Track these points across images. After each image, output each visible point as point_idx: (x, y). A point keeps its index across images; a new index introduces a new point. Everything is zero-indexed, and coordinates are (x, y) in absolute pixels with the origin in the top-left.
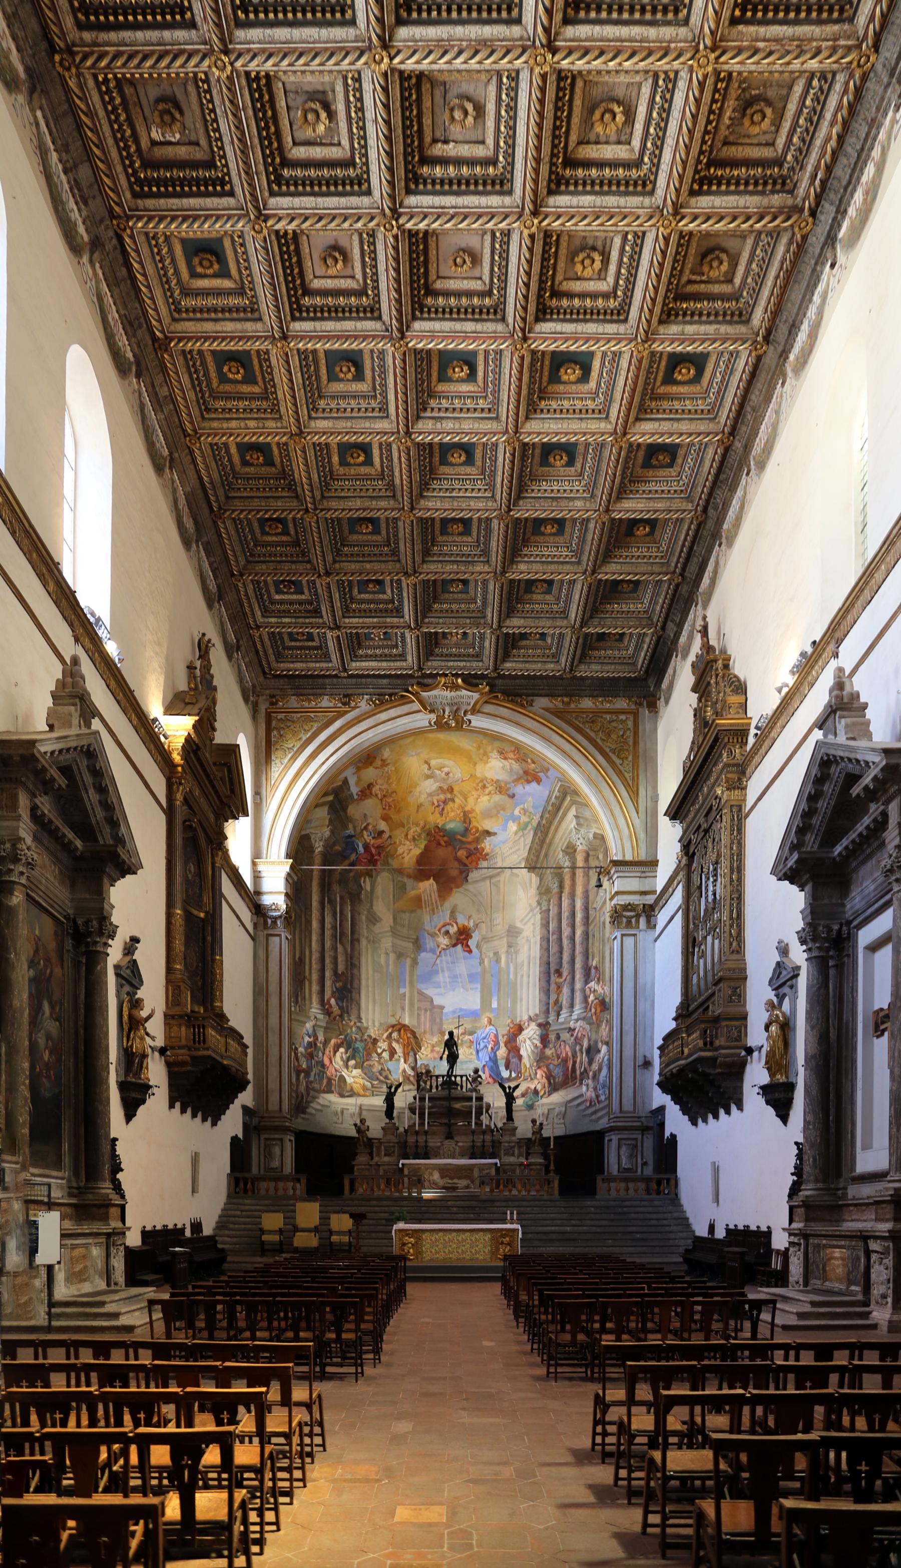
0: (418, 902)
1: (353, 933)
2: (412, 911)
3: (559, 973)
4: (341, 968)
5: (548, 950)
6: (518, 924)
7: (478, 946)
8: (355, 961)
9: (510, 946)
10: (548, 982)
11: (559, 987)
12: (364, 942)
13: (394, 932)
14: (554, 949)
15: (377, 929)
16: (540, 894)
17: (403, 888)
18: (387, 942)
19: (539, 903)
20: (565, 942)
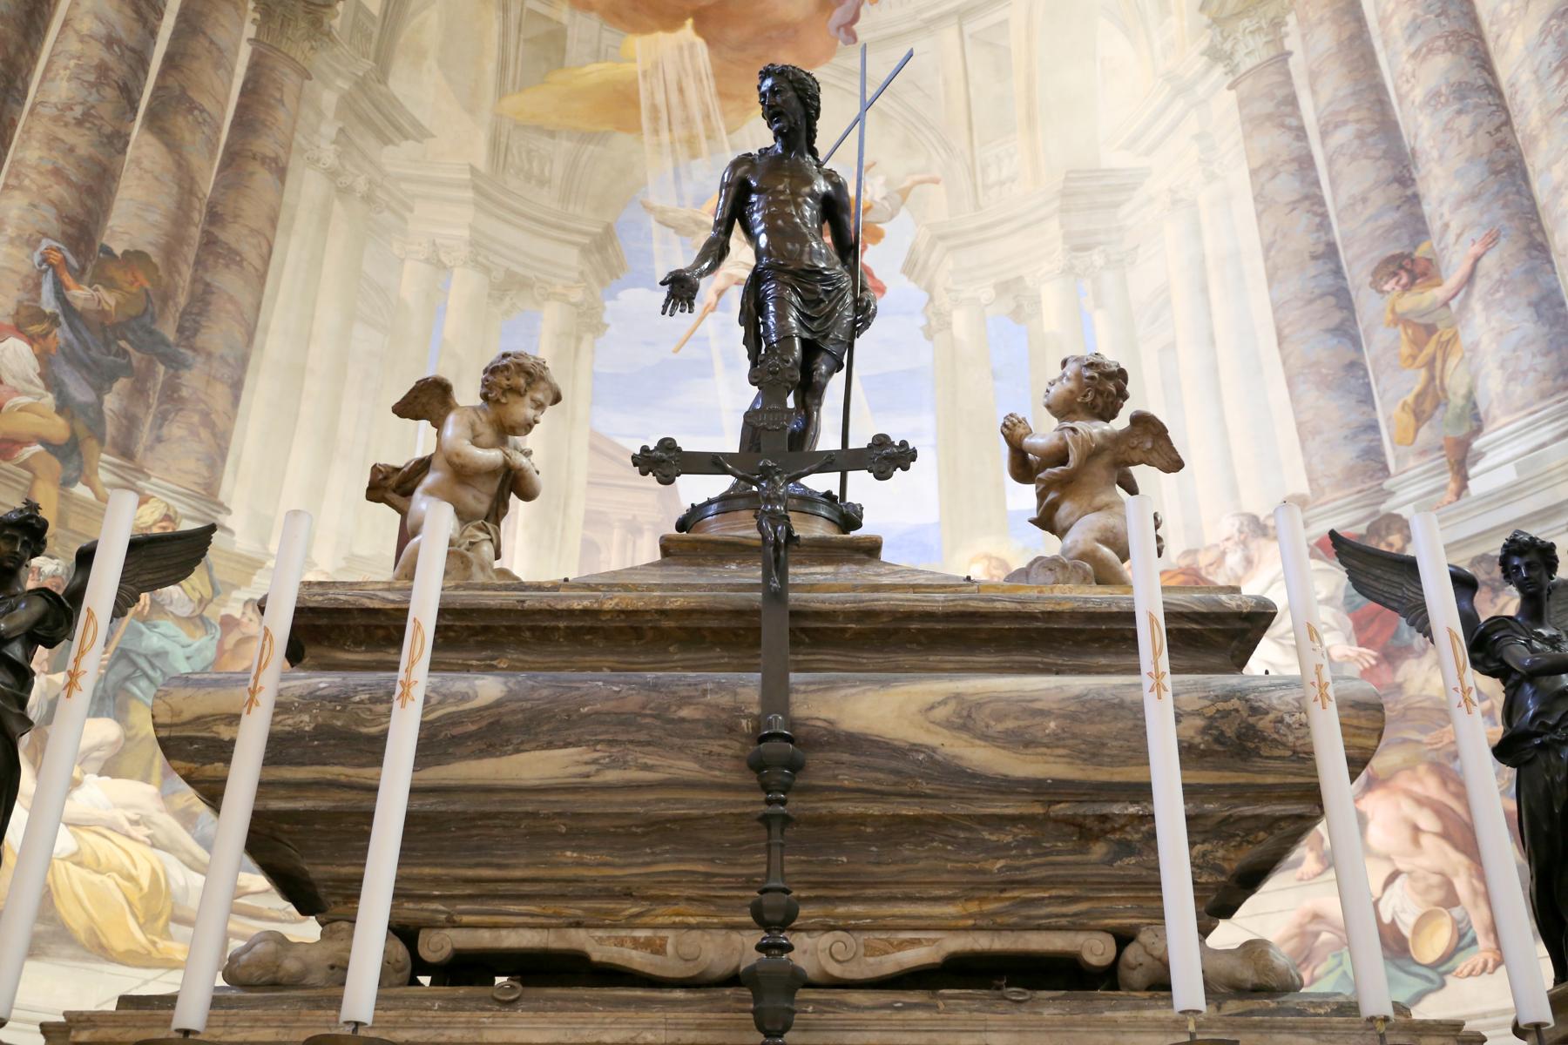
0: (621, 105)
1: (246, 121)
2: (587, 137)
3: (1408, 267)
4: (132, 220)
5: (1313, 200)
6: (1114, 159)
7: (911, 268)
8: (229, 235)
9: (1079, 245)
10: (1346, 330)
11: (1428, 336)
12: (307, 188)
13: (485, 191)
14: (1349, 182)
15: (396, 158)
16: (1215, 21)
17: (552, 45)
18: (449, 222)
19: (1215, 55)
20: (1422, 126)
